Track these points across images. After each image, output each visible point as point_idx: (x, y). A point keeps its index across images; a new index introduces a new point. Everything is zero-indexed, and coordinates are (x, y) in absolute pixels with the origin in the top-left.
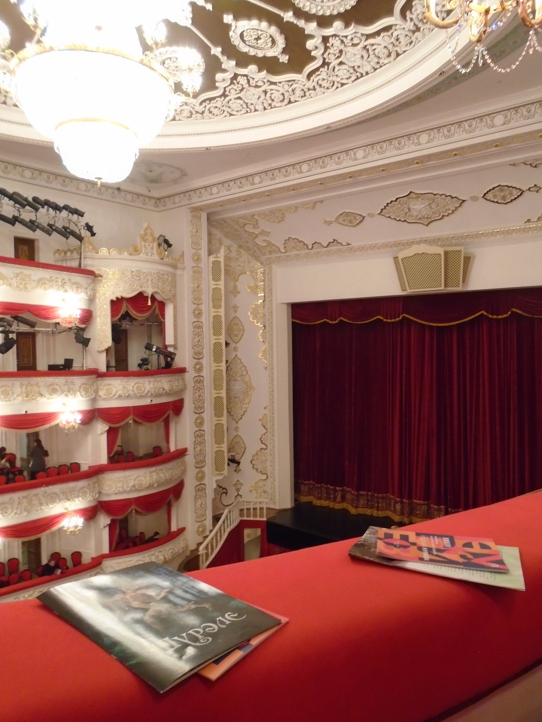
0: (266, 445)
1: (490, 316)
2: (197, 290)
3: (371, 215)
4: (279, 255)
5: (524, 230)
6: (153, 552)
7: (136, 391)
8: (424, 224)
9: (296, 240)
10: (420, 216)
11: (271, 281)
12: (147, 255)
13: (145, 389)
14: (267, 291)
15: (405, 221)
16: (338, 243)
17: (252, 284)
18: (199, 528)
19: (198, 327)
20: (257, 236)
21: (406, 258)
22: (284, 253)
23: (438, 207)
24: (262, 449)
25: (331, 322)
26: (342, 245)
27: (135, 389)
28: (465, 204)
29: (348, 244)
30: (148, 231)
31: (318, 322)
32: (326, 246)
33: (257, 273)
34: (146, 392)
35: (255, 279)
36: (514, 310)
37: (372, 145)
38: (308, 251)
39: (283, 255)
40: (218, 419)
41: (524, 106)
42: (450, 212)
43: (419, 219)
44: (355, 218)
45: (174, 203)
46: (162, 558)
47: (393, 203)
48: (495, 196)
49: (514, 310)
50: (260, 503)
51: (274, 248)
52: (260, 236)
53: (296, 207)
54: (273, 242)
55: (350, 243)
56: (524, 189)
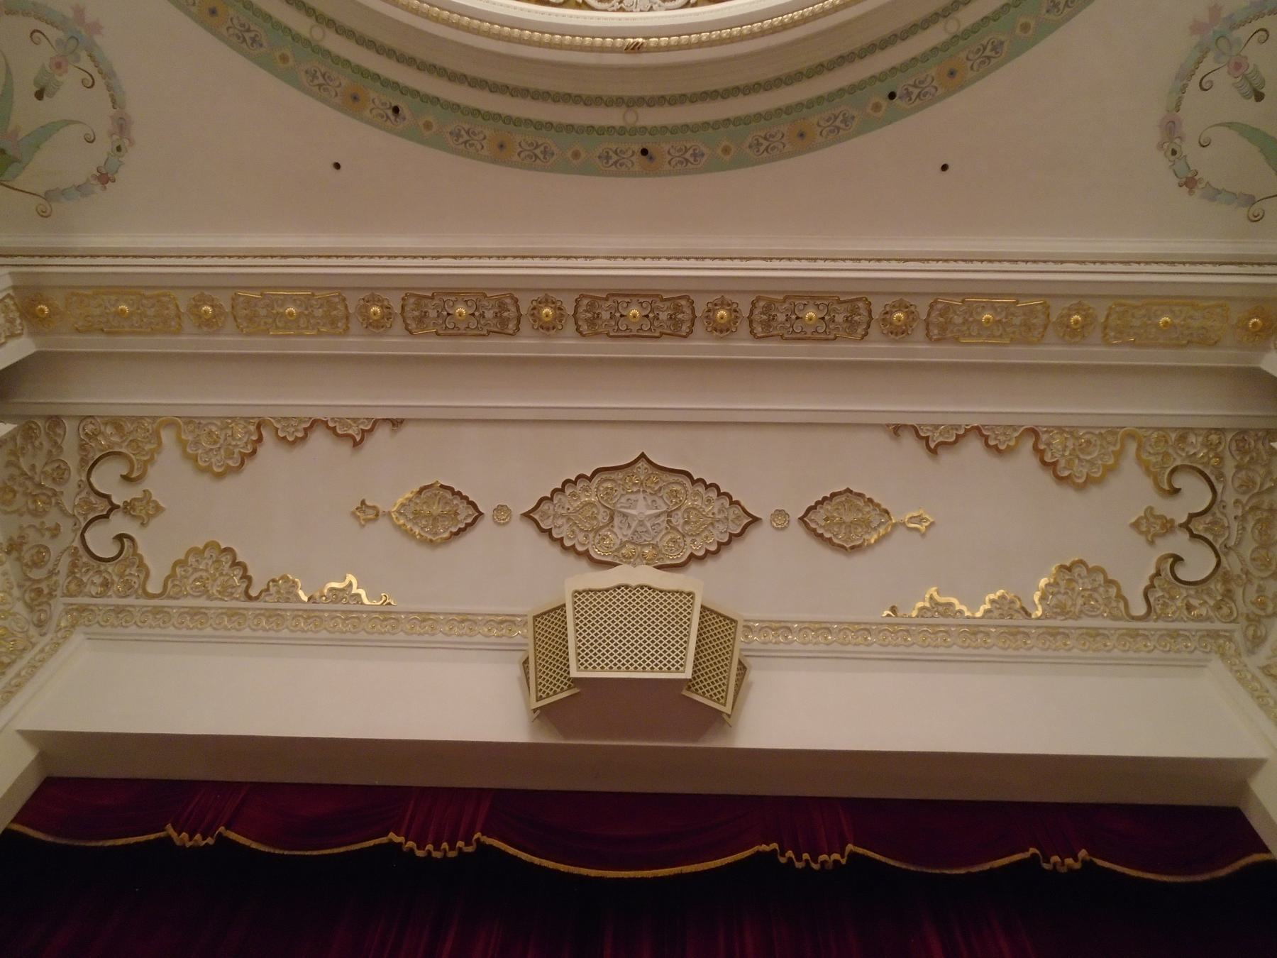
9: (226, 559)
21: (587, 592)
23: (687, 528)
28: (755, 535)
42: (713, 548)
51: (134, 571)
53: (315, 423)
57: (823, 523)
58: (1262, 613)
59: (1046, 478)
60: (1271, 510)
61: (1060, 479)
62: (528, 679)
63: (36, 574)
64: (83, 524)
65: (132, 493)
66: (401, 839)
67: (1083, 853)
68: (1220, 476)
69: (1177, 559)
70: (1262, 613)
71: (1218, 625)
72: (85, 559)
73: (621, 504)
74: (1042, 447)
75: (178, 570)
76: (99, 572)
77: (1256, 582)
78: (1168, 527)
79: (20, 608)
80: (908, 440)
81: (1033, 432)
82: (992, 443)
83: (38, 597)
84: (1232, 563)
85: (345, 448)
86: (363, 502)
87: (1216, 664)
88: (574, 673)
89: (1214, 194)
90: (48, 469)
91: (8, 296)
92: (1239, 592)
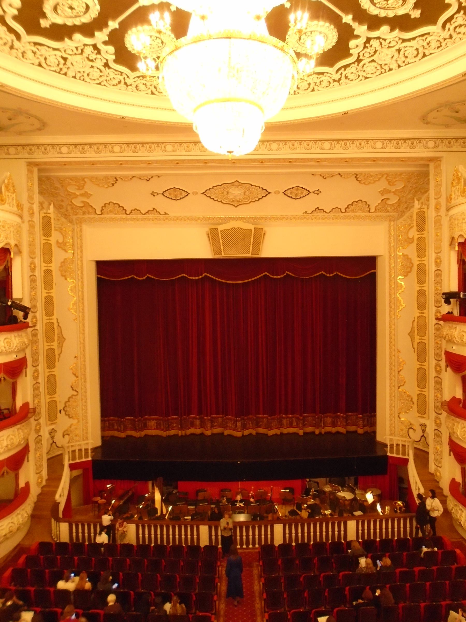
0: (77, 392)
2: (31, 244)
3: (195, 193)
4: (93, 216)
5: (301, 218)
6: (18, 512)
7: (7, 347)
8: (234, 206)
9: (116, 205)
10: (234, 199)
11: (81, 240)
12: (10, 206)
13: (13, 344)
14: (76, 249)
15: (221, 201)
16: (157, 212)
17: (61, 241)
18: (38, 480)
19: (33, 280)
20: (76, 196)
21: (224, 230)
22: (99, 215)
24: (73, 395)
25: (139, 278)
27: (6, 345)
29: (166, 214)
30: (10, 181)
31: (124, 278)
33: (65, 231)
34: (15, 347)
35: (64, 237)
36: (287, 272)
38: (125, 216)
39: (96, 216)
41: (342, 140)
43: (233, 201)
44: (181, 194)
45: (8, 154)
46: (26, 515)
48: (291, 193)
49: (287, 272)
50: (72, 446)
51: (90, 209)
53: (133, 177)
54: (90, 204)
55: (167, 213)
56: (310, 191)
58: (405, 210)
59: (358, 182)
63: (61, 211)
65: (82, 192)
68: (409, 181)
70: (405, 210)
73: (231, 191)
74: (358, 177)
76: (81, 210)
77: (408, 204)
78: (390, 192)
79: (63, 219)
83: (66, 216)
85: (145, 181)
86: (153, 192)
87: (387, 223)
90: (52, 187)
91: (27, 165)
92: (402, 206)
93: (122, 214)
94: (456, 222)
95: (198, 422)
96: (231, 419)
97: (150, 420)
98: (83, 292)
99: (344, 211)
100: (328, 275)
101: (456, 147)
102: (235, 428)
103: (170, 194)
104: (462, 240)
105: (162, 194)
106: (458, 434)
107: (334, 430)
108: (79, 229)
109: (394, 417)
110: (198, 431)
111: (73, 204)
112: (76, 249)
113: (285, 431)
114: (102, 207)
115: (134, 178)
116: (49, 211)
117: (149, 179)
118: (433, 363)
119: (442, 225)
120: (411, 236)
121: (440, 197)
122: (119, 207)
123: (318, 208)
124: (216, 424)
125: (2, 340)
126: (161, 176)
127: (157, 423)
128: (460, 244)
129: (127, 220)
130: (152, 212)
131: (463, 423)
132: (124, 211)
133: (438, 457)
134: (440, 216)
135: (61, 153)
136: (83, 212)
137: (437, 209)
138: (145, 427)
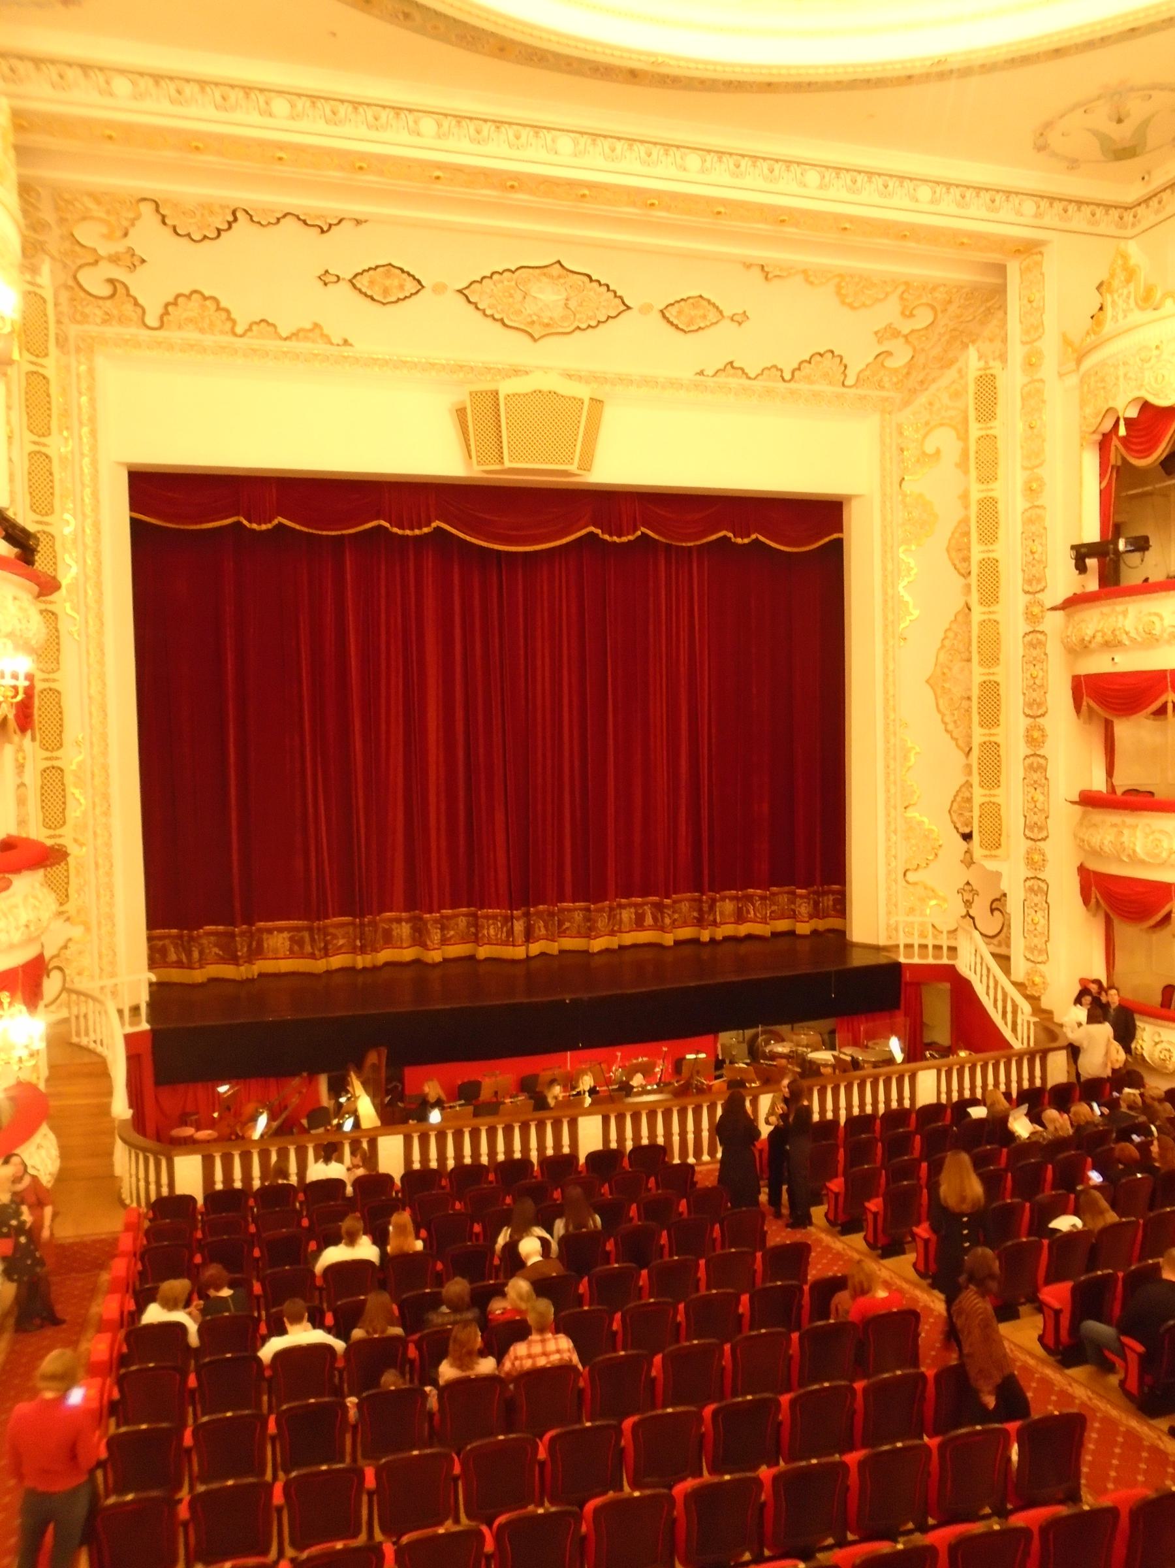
1: (606, 537)
3: (439, 289)
8: (532, 336)
9: (208, 303)
10: (535, 318)
11: (92, 401)
25: (255, 526)
26: (332, 344)
29: (346, 342)
32: (284, 335)
37: (595, 136)
40: (48, 754)
42: (593, 323)
43: (533, 322)
44: (401, 287)
47: (506, 274)
48: (680, 312)
49: (643, 529)
51: (128, 308)
52: (103, 264)
55: (350, 341)
56: (727, 313)
57: (674, 313)
58: (918, 388)
60: (962, 332)
61: (843, 303)
62: (468, 446)
64: (74, 267)
65: (119, 247)
66: (387, 525)
67: (754, 536)
68: (944, 311)
69: (889, 354)
70: (918, 388)
71: (892, 394)
72: (82, 294)
73: (534, 289)
75: (170, 309)
76: (100, 307)
78: (896, 334)
80: (756, 271)
81: (841, 276)
82: (812, 279)
84: (921, 359)
86: (327, 272)
88: (508, 464)
89: (1054, 154)
93: (222, 332)
94: (1121, 373)
95: (405, 930)
96: (495, 917)
97: (270, 931)
98: (97, 554)
99: (787, 376)
100: (739, 541)
101: (1079, 220)
102: (508, 936)
103: (372, 283)
104: (1133, 413)
105: (350, 281)
106: (1138, 849)
107: (743, 930)
108: (83, 368)
109: (896, 881)
110: (408, 954)
111: (81, 287)
112: (76, 424)
113: (628, 939)
114: (167, 305)
115: (289, 218)
116: (39, 280)
117: (330, 225)
118: (1022, 723)
119: (1044, 402)
120: (930, 448)
121: (1040, 337)
122: (219, 308)
123: (731, 363)
124: (452, 933)
125: (10, 598)
126: (366, 221)
127: (291, 939)
128: (1129, 422)
129: (235, 352)
130: (311, 335)
131: (1148, 825)
132: (229, 325)
133: (1036, 941)
134: (1042, 381)
135: (111, 94)
136: (107, 314)
137: (1031, 364)
138: (256, 952)
